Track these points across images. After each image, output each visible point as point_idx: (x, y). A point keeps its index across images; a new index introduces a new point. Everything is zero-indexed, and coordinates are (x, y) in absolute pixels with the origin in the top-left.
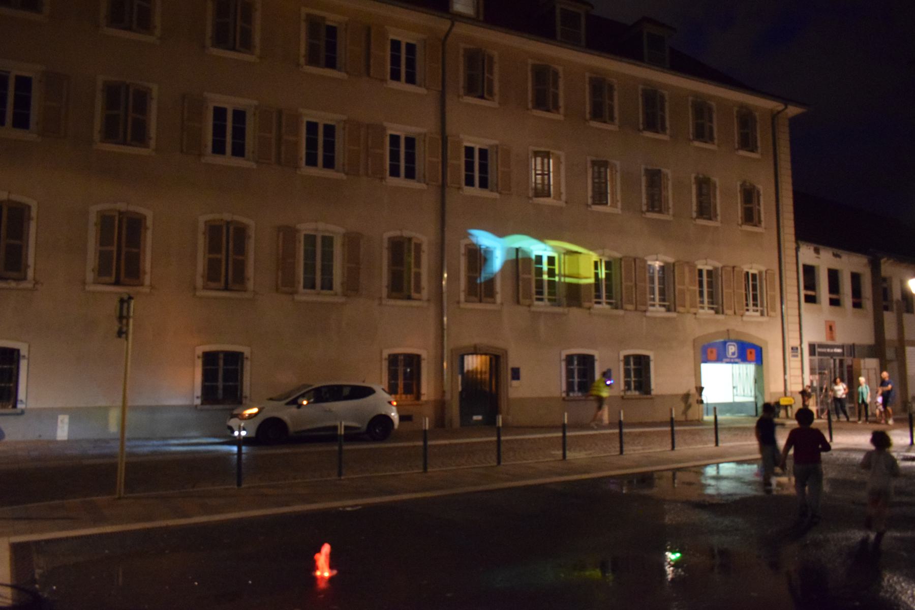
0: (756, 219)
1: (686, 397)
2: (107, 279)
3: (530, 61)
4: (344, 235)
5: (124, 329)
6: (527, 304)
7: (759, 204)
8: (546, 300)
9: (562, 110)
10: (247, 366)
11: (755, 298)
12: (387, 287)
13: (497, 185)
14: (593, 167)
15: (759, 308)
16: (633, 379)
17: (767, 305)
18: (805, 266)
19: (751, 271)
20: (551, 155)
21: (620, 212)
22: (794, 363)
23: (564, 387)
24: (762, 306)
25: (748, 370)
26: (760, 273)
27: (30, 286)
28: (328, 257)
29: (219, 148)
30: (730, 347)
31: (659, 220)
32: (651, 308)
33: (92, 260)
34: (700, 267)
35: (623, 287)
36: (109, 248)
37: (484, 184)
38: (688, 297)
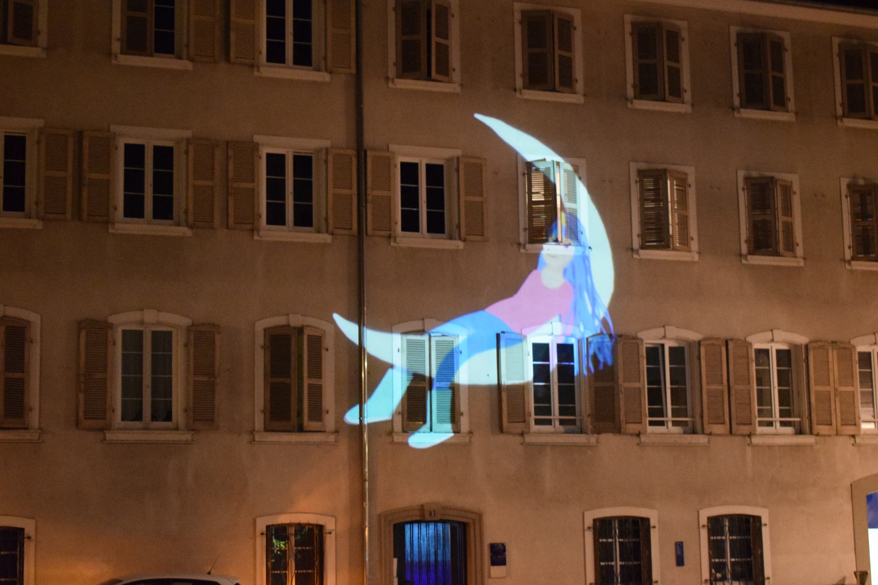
4: (189, 329)
6: (519, 431)
8: (557, 423)
9: (580, 86)
12: (264, 412)
13: (459, 227)
14: (641, 183)
16: (729, 560)
21: (696, 258)
28: (163, 364)
32: (760, 429)
37: (436, 225)
38: (836, 406)
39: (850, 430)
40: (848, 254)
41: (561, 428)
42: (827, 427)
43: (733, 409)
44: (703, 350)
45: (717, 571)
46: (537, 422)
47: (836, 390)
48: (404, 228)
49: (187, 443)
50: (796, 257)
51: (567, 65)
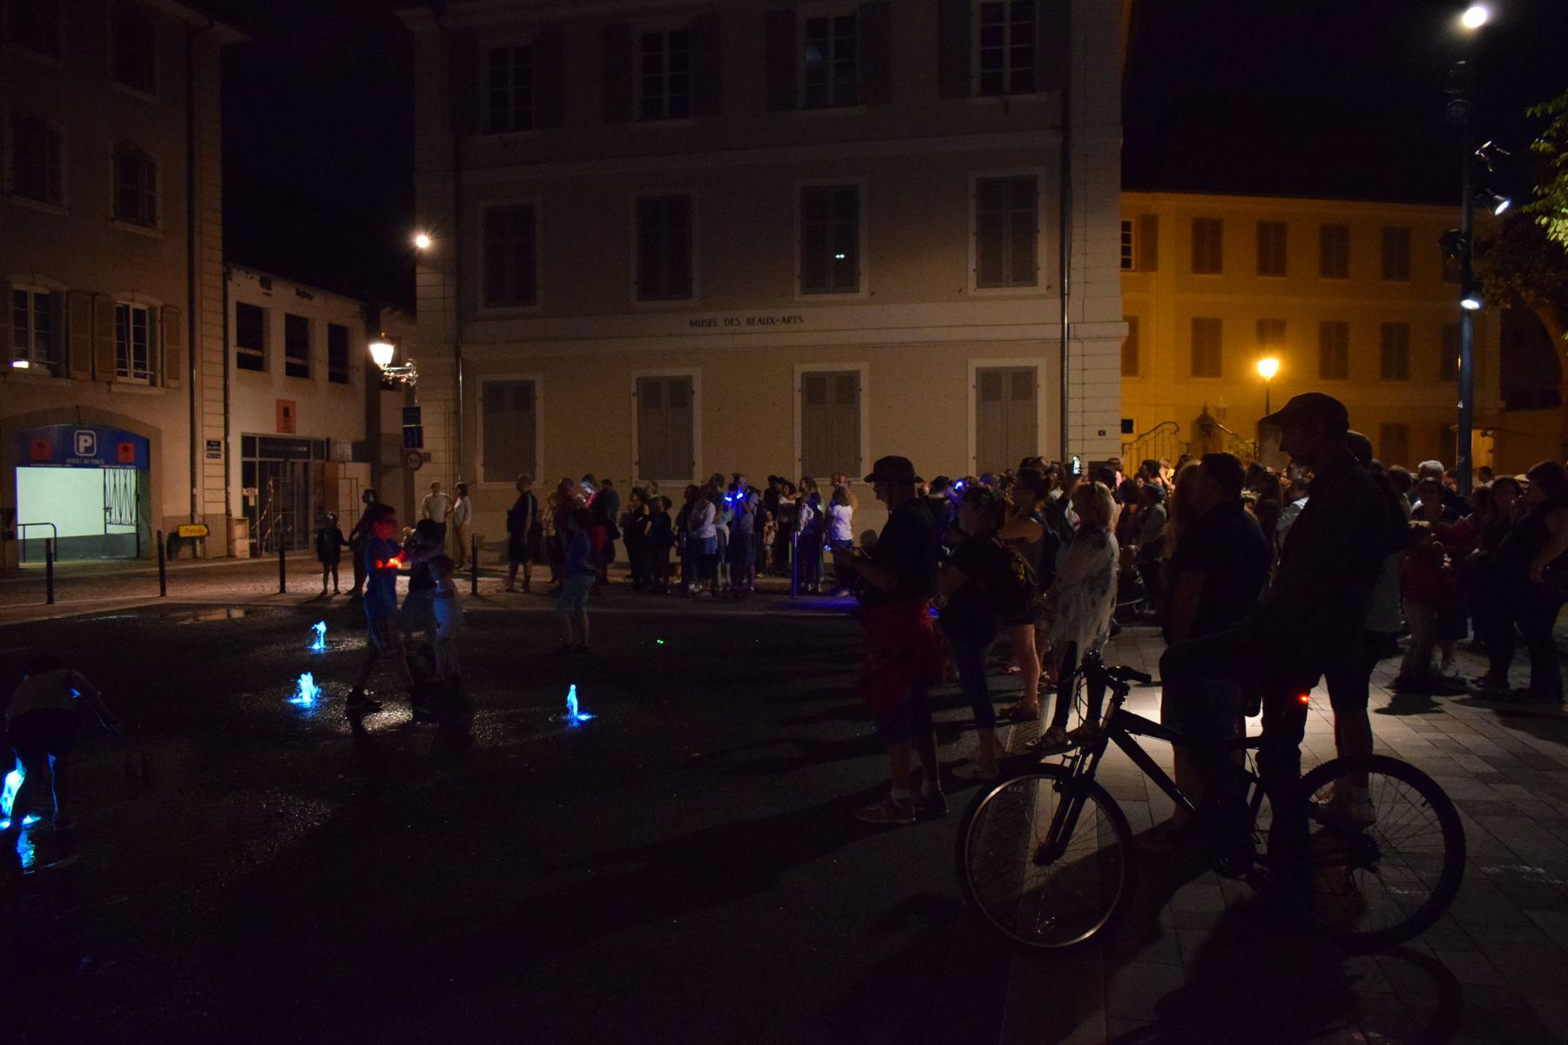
17: (162, 368)
18: (241, 308)
19: (133, 306)
22: (211, 469)
24: (153, 368)
25: (126, 478)
26: (152, 309)
30: (82, 438)
34: (19, 286)
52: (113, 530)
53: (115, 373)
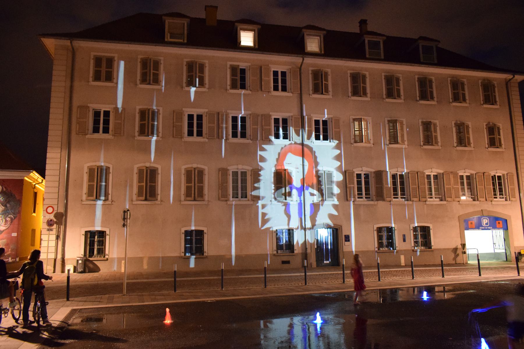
0: (497, 143)
1: (455, 250)
2: (141, 198)
3: (349, 72)
4: (251, 171)
5: (126, 224)
7: (499, 135)
8: (364, 198)
9: (369, 95)
10: (206, 237)
11: (501, 190)
14: (389, 124)
15: (504, 196)
19: (497, 175)
20: (363, 120)
23: (376, 245)
25: (500, 233)
26: (503, 175)
27: (110, 203)
29: (190, 134)
30: (484, 220)
31: (431, 149)
32: (429, 199)
33: (135, 190)
35: (411, 188)
36: (142, 184)
38: (453, 192)
39: (458, 199)
40: (455, 145)
41: (366, 199)
42: (451, 199)
43: (420, 193)
44: (410, 175)
45: (416, 244)
46: (358, 198)
47: (453, 187)
48: (316, 139)
49: (252, 205)
50: (438, 146)
51: (364, 89)
52: (497, 251)
53: (493, 198)
